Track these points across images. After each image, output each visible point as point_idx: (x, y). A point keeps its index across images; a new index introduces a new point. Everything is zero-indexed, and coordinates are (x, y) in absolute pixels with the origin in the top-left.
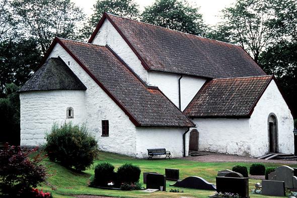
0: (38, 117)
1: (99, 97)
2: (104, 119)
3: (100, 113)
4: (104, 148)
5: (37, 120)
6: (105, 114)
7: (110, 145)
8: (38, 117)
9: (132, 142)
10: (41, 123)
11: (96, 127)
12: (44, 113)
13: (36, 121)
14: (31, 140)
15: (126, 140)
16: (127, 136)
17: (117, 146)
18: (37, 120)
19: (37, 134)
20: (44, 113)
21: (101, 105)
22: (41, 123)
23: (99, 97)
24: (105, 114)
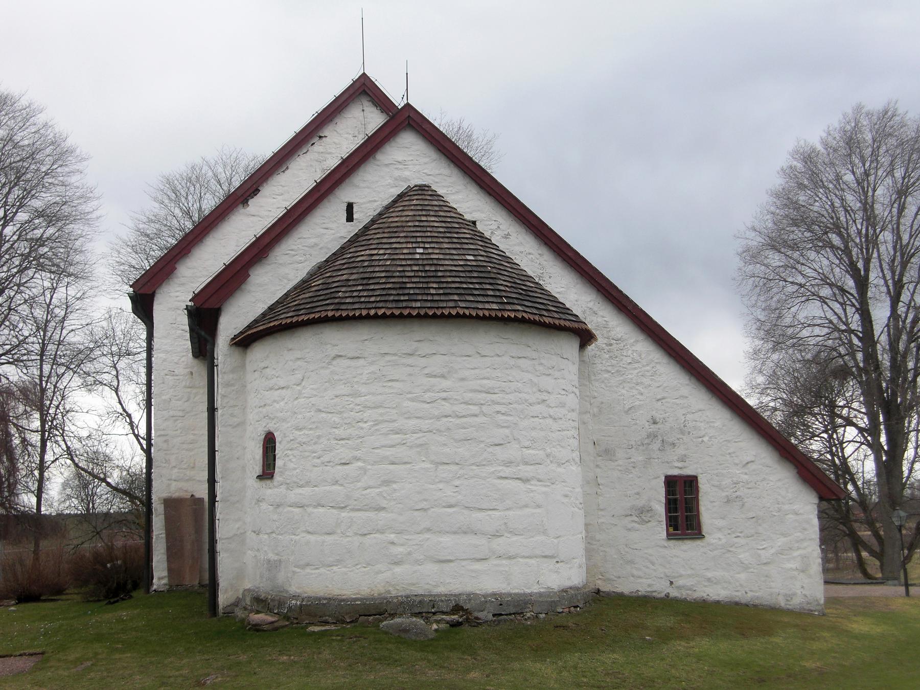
0: (512, 451)
1: (646, 381)
2: (676, 472)
3: (656, 445)
4: (679, 588)
5: (508, 463)
6: (680, 451)
7: (709, 575)
8: (512, 451)
9: (804, 557)
10: (525, 481)
11: (640, 503)
12: (534, 434)
13: (507, 471)
14: (477, 566)
15: (781, 552)
16: (784, 535)
17: (743, 576)
18: (508, 463)
19: (513, 533)
20: (534, 434)
21: (658, 416)
22: (525, 481)
23: (646, 381)
24: (680, 451)
